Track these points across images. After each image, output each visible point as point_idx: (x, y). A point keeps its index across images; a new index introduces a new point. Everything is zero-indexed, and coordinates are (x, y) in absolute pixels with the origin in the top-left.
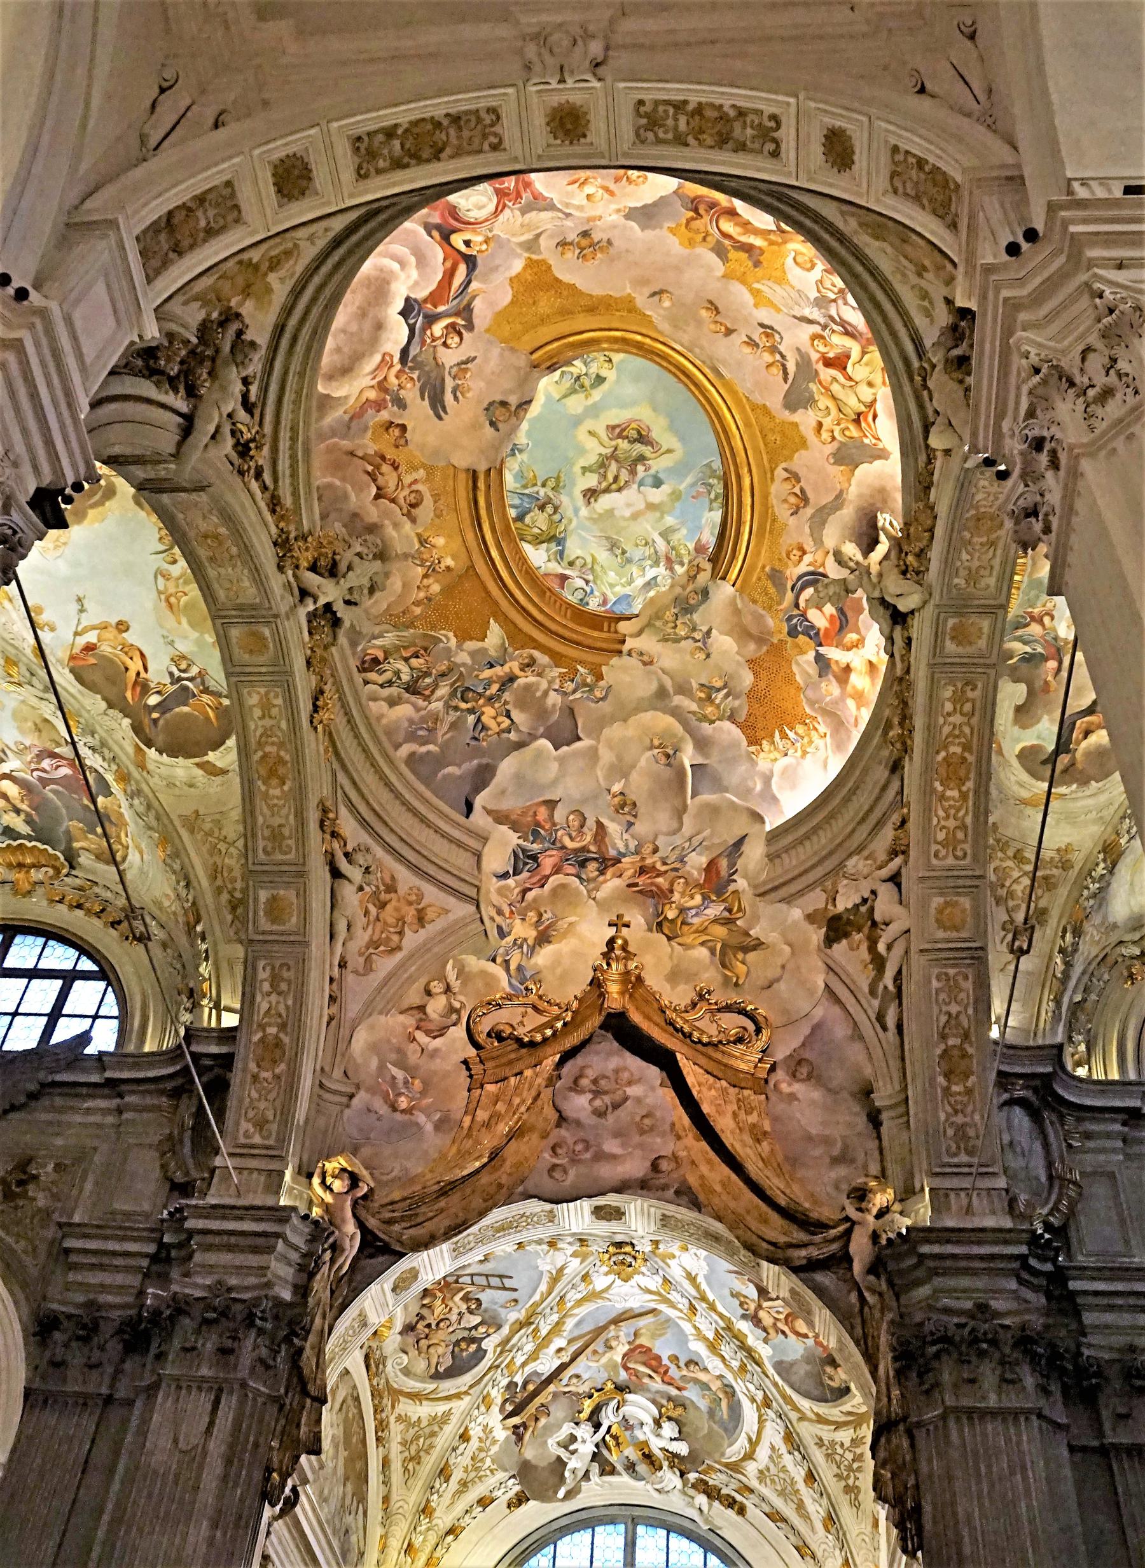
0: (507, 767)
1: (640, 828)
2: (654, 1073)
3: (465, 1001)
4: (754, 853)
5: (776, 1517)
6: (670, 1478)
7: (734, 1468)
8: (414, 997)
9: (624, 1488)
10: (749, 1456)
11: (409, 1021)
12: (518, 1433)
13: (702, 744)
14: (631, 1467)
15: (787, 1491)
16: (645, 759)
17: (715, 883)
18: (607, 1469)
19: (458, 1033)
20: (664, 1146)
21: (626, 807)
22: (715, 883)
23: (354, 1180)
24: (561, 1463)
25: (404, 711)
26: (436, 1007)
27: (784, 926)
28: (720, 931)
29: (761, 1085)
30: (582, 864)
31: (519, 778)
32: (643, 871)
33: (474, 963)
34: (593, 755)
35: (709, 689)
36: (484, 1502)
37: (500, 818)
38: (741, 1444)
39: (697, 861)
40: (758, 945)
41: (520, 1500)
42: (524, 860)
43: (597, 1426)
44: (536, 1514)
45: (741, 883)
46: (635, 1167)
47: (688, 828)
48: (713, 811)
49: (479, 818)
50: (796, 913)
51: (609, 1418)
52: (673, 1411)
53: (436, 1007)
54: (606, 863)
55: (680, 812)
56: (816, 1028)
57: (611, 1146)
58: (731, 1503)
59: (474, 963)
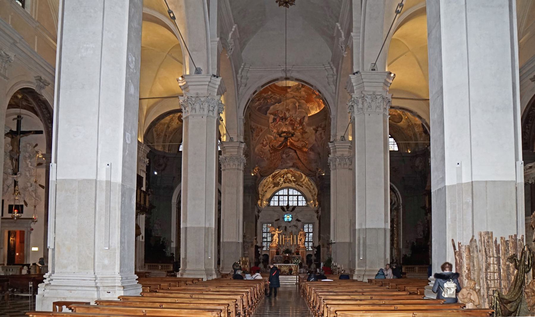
0: (272, 107)
1: (291, 113)
2: (293, 151)
3: (268, 142)
4: (306, 119)
5: (307, 188)
6: (294, 184)
7: (302, 182)
8: (261, 142)
9: (287, 185)
10: (304, 181)
11: (261, 145)
12: (273, 180)
13: (299, 103)
14: (288, 182)
15: (308, 185)
16: (291, 104)
17: (301, 123)
18: (285, 183)
19: (268, 146)
20: (295, 161)
21: (288, 110)
22: (301, 123)
23: (259, 169)
24: (279, 182)
25: (257, 103)
26: (265, 143)
27: (310, 130)
28: (301, 130)
29: (306, 152)
30: (282, 119)
31: (273, 108)
32: (291, 120)
33: (269, 136)
34: (284, 104)
35: (301, 97)
36: (269, 188)
37: (271, 114)
38: (302, 180)
39: (298, 119)
40: (306, 132)
41: (274, 187)
42: (274, 120)
43: (283, 177)
44: (276, 188)
45: (304, 123)
46: (291, 164)
47: (297, 113)
48: (301, 112)
49: (268, 115)
50: (312, 128)
51: (285, 177)
52: (293, 175)
53: (265, 143)
54: (286, 119)
55: (296, 111)
56: (314, 145)
57: (288, 161)
58: (301, 186)
59: (269, 136)
